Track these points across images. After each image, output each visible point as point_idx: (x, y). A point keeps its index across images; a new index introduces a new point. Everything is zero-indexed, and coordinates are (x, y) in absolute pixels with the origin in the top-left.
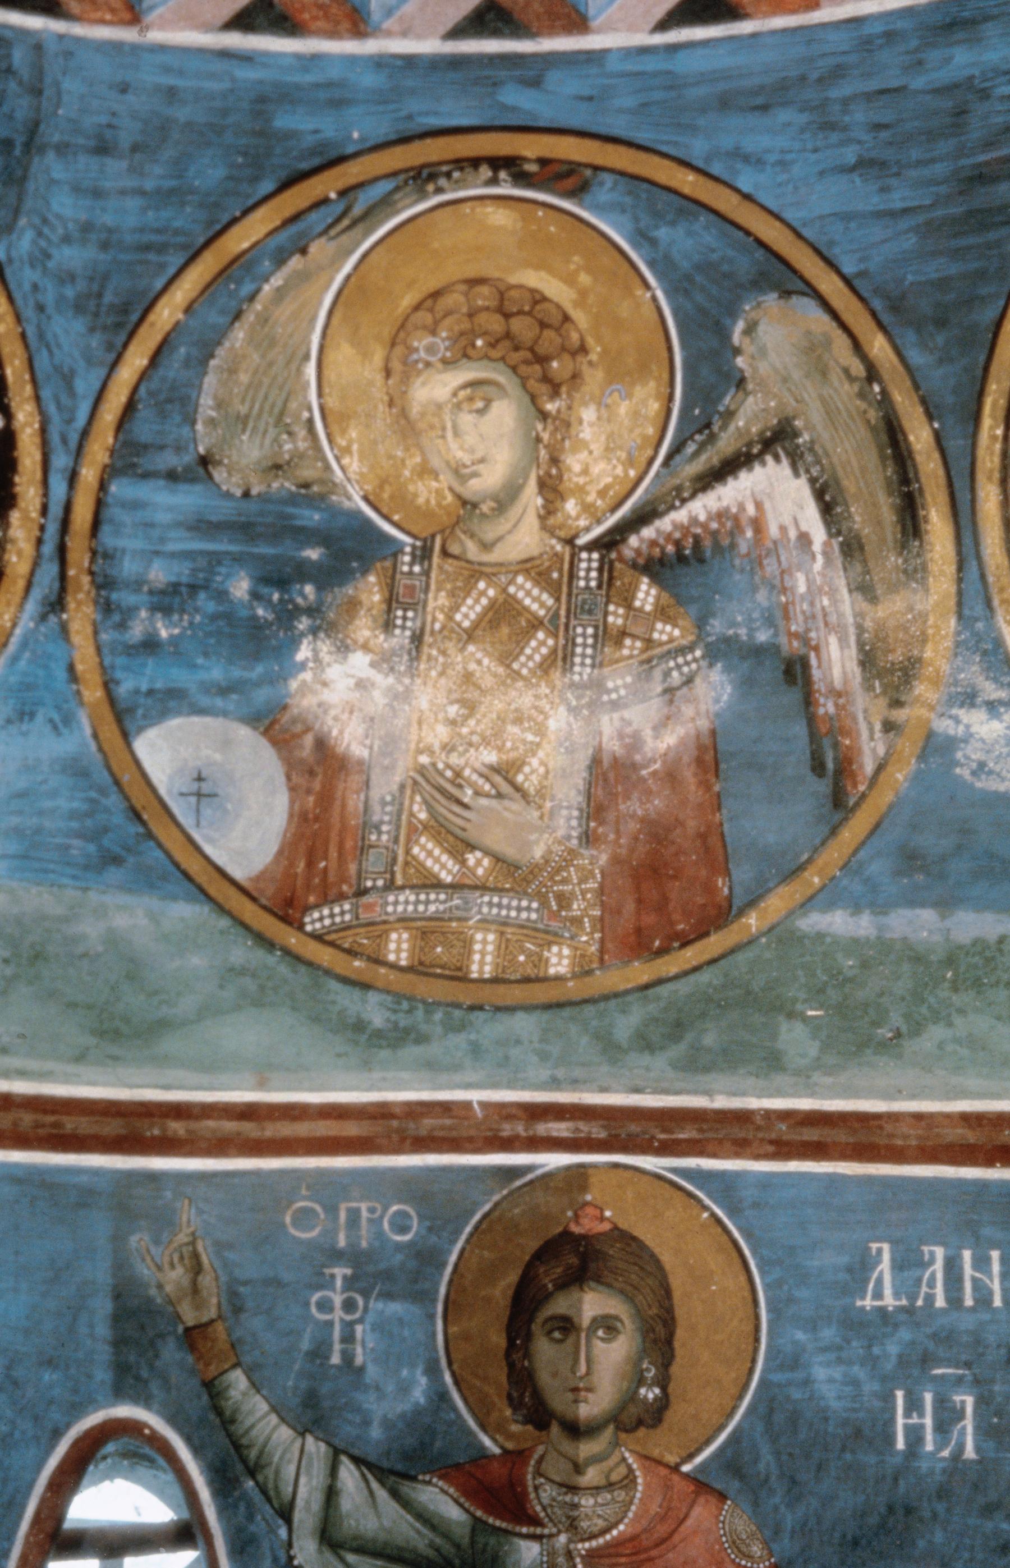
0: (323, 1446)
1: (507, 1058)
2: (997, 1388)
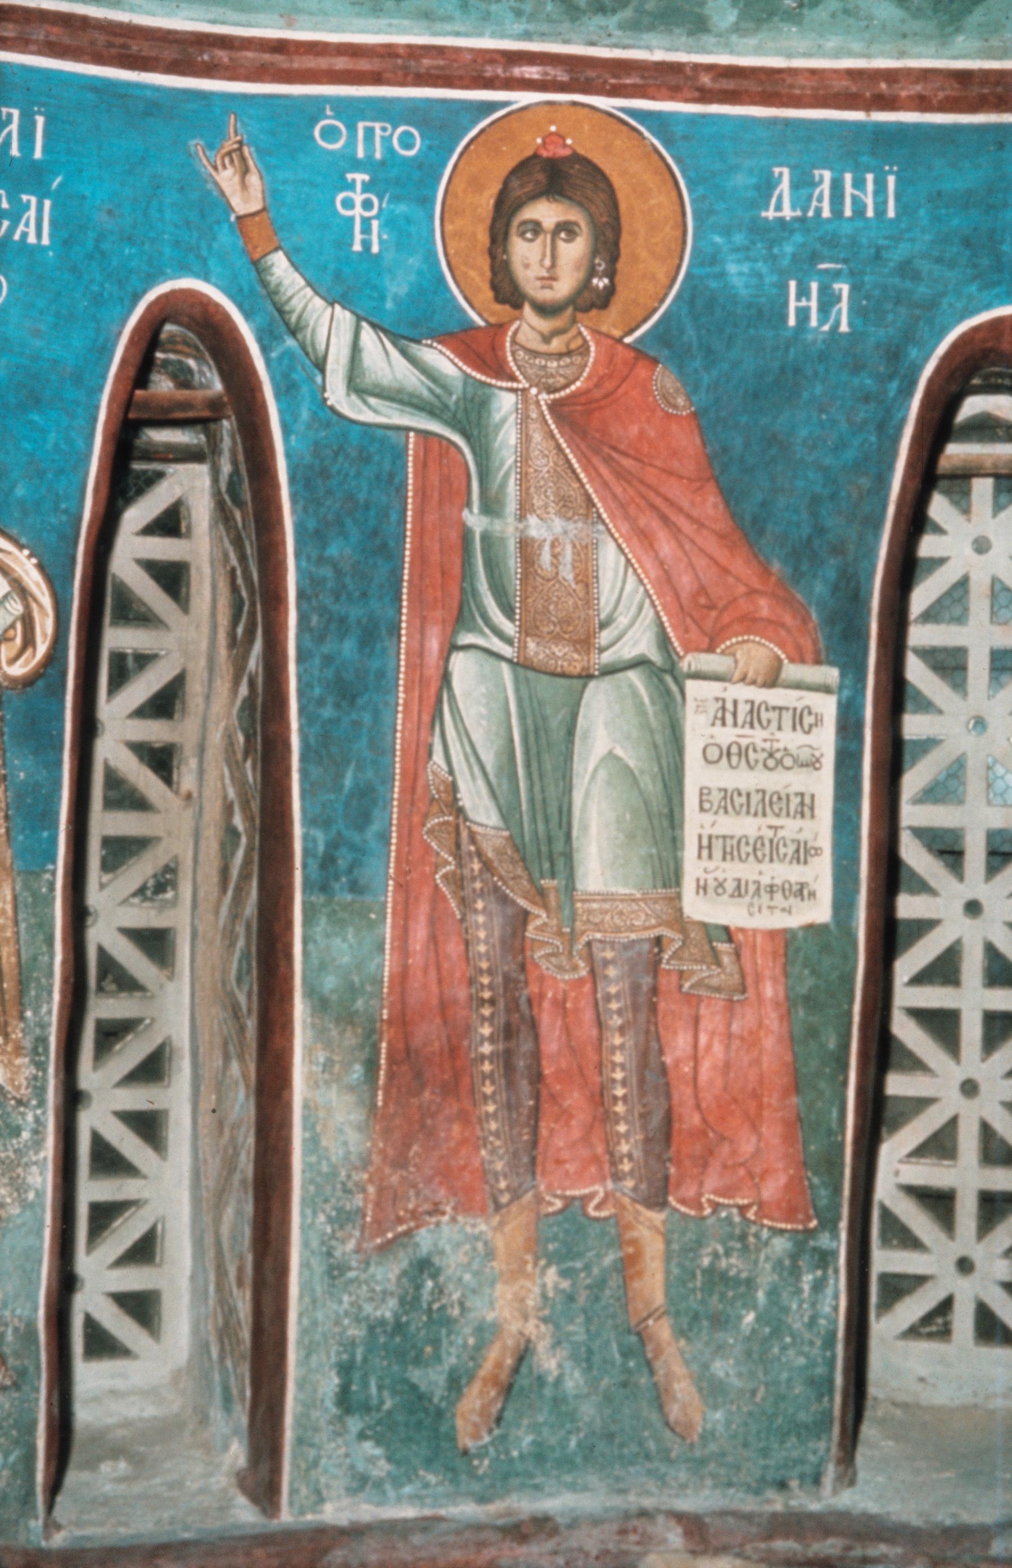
1: (489, 13)
2: (867, 278)
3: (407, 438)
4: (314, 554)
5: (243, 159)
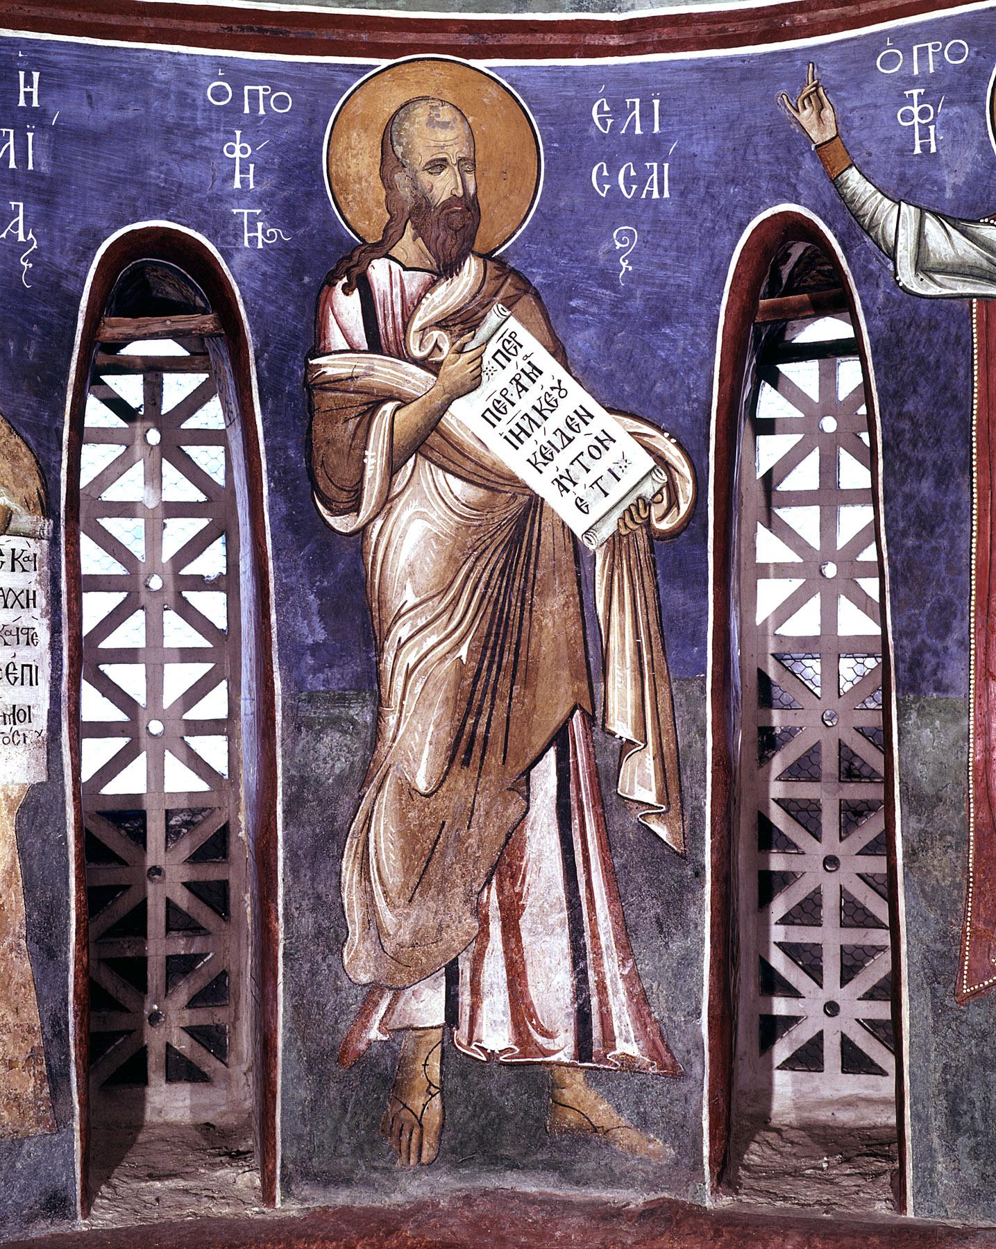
0: (912, 208)
3: (971, 304)
4: (895, 410)
5: (820, 98)
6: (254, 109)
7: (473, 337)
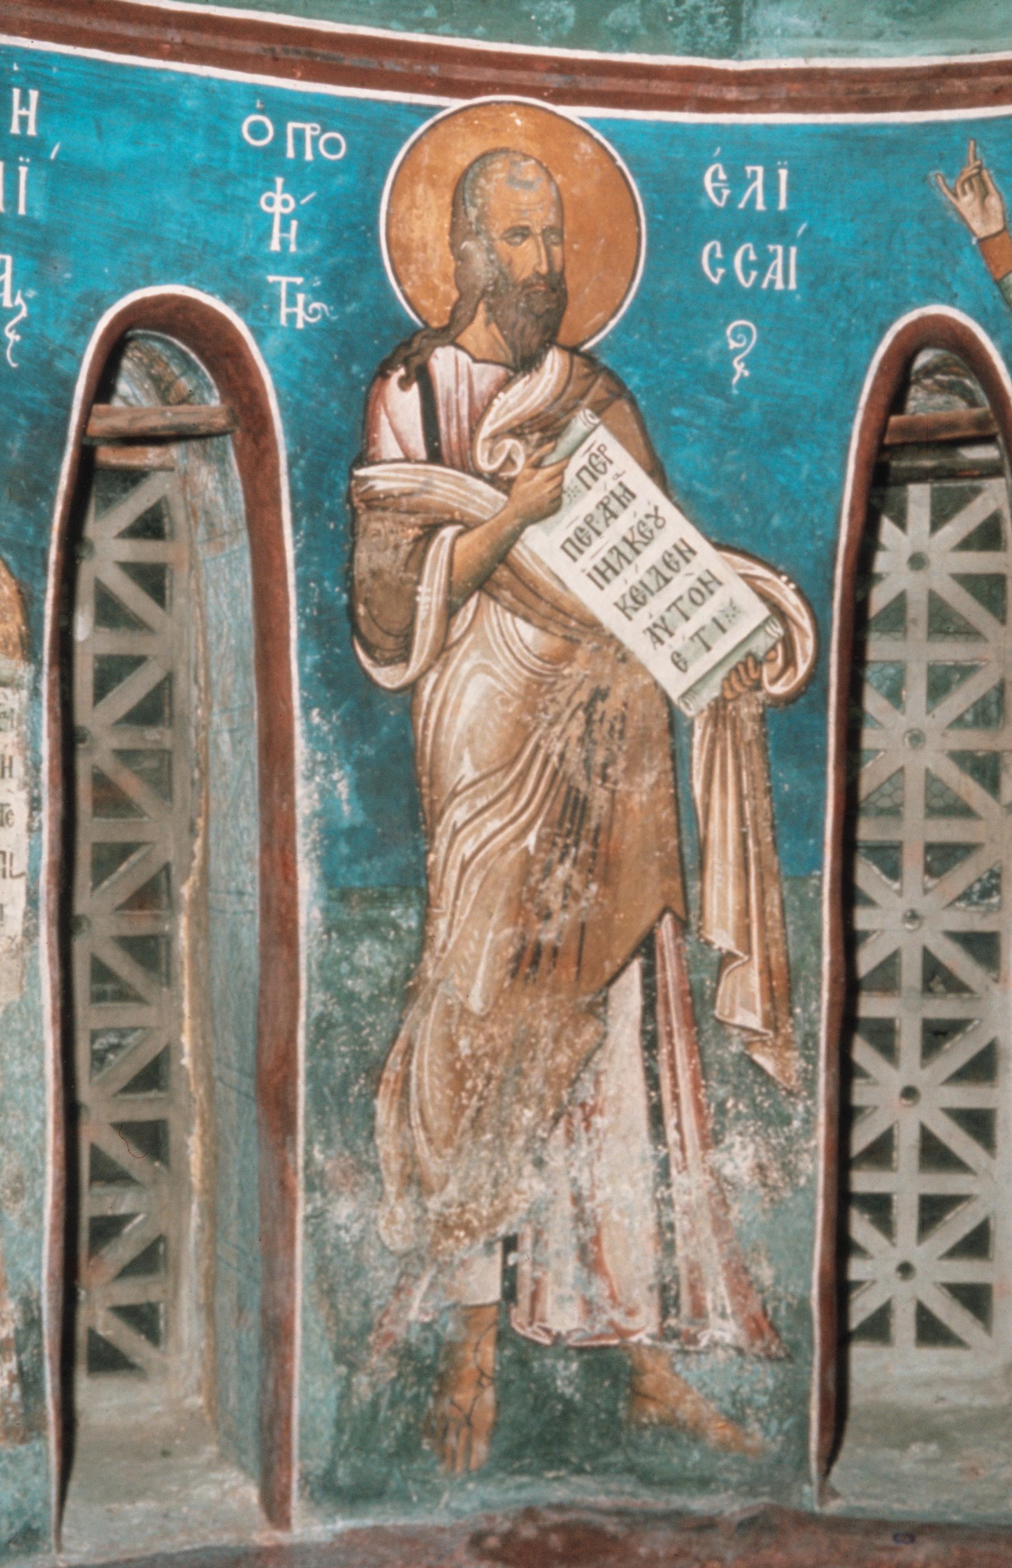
5: (983, 183)
6: (300, 151)
7: (554, 449)
